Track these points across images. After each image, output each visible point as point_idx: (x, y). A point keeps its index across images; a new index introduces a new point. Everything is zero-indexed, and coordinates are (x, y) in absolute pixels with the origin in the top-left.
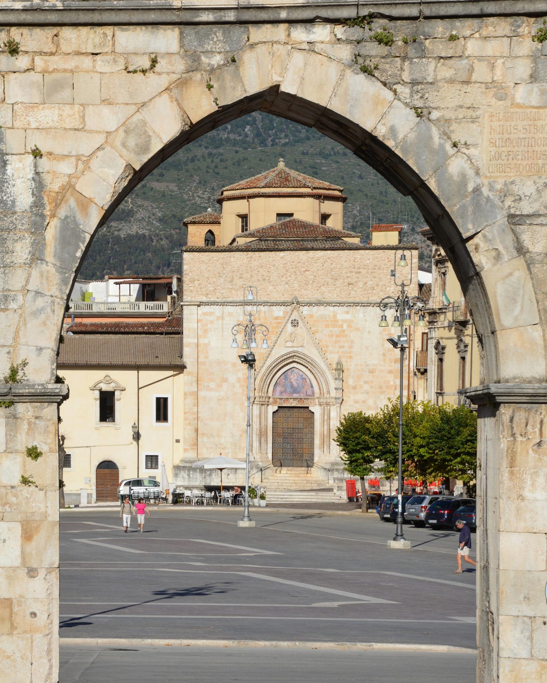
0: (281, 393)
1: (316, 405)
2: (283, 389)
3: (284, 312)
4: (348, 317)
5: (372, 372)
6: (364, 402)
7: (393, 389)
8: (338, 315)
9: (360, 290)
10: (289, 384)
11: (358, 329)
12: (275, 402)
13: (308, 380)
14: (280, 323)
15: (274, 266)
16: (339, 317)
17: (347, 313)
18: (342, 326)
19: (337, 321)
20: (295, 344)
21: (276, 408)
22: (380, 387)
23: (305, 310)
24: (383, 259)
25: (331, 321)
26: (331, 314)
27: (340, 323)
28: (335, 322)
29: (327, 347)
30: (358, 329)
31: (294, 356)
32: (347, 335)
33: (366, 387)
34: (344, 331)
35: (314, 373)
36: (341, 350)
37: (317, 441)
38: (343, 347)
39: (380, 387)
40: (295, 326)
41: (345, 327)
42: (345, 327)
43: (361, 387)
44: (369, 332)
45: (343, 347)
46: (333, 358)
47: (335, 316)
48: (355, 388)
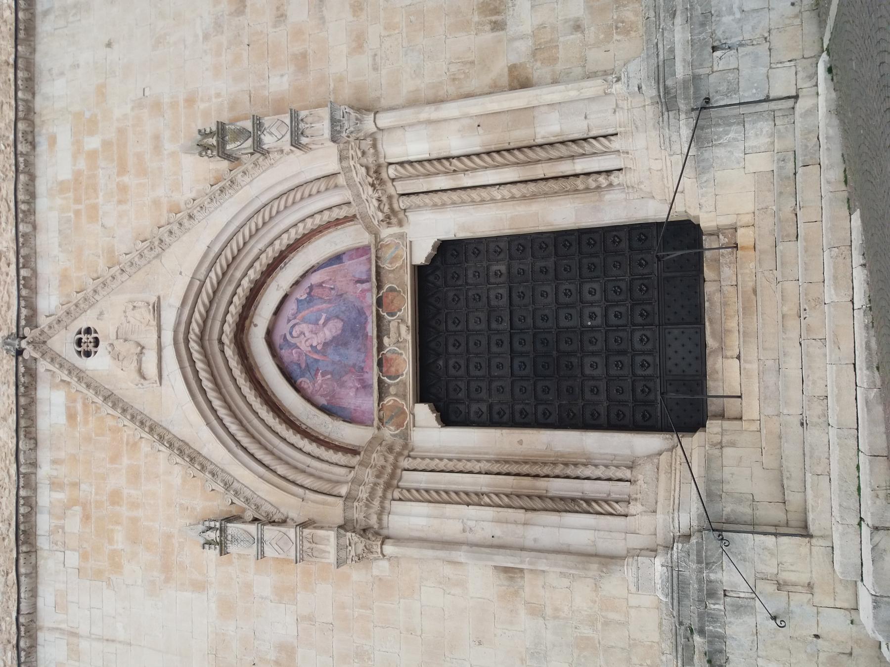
0: (365, 386)
1: (402, 236)
2: (351, 381)
3: (53, 386)
4: (64, 139)
8: (60, 178)
10: (333, 356)
11: (101, 92)
12: (399, 416)
14: (85, 405)
17: (53, 140)
18: (92, 155)
19: (78, 174)
20: (150, 340)
21: (424, 413)
23: (49, 302)
25: (77, 201)
26: (59, 201)
27: (82, 164)
28: (80, 186)
29: (156, 203)
30: (101, 92)
31: (201, 339)
32: (121, 131)
34: (106, 144)
35: (271, 253)
36: (169, 146)
37: (562, 214)
38: (157, 138)
40: (97, 342)
41: (93, 143)
42: (93, 143)
43: (298, 33)
44: (109, 45)
45: (157, 138)
47: (62, 187)
48: (301, 61)
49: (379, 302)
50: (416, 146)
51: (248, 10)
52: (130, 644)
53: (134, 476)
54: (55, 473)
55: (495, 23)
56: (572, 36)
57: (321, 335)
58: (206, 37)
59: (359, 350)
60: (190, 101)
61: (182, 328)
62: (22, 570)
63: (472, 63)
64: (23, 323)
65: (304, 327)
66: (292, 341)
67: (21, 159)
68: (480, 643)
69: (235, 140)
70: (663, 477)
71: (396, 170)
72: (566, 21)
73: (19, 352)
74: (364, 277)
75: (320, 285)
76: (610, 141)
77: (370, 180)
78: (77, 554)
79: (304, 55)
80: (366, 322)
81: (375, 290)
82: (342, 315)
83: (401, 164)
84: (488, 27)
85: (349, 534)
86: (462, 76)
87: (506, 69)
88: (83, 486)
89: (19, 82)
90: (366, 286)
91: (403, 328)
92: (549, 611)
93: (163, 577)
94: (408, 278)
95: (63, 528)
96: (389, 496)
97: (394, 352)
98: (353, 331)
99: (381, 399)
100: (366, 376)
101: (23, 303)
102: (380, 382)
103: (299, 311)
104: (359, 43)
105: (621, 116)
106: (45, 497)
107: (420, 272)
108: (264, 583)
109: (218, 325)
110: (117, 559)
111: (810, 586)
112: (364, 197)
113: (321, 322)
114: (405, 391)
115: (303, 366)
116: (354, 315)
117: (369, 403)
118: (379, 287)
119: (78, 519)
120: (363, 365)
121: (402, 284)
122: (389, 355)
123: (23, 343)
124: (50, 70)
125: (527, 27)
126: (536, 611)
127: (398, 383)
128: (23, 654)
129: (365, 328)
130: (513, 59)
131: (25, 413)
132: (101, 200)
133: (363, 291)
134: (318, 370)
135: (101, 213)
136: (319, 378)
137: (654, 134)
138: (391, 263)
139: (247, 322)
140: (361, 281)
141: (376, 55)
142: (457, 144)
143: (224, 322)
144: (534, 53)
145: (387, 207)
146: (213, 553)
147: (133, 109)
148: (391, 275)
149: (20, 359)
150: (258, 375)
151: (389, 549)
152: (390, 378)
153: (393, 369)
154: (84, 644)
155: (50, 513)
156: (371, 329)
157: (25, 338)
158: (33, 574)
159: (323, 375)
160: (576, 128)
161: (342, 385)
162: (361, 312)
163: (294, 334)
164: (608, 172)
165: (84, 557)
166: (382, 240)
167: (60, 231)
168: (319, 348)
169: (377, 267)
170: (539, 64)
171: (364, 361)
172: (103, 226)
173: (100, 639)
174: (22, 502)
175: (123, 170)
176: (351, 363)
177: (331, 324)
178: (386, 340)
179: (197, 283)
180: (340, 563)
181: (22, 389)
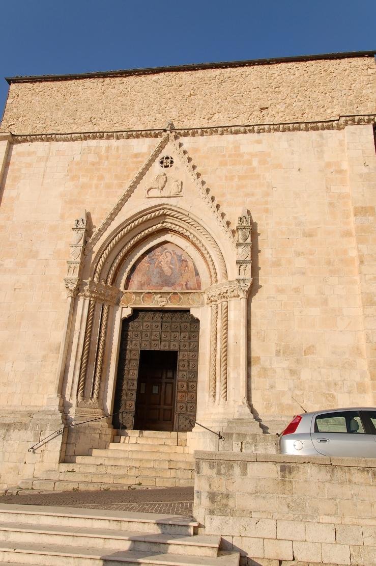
0: (142, 285)
1: (203, 304)
2: (144, 279)
4: (258, 148)
5: (310, 235)
6: (297, 290)
7: (357, 263)
8: (241, 147)
9: (281, 114)
10: (156, 270)
13: (190, 264)
15: (142, 92)
16: (243, 149)
17: (259, 142)
18: (249, 162)
20: (164, 193)
21: (127, 312)
22: (329, 263)
23: (186, 141)
24: (317, 72)
25: (230, 156)
27: (246, 157)
29: (223, 195)
33: (300, 262)
34: (253, 170)
39: (329, 263)
42: (255, 163)
46: (234, 214)
47: (237, 148)
48: (276, 264)
49: (175, 293)
50: (232, 315)
51: (305, 238)
52: (42, 185)
53: (108, 186)
54: (113, 148)
55: (279, 352)
56: (268, 385)
57: (166, 266)
58: (295, 218)
59: (157, 283)
60: (267, 211)
61: (168, 207)
62: (73, 135)
63: (264, 341)
64: (178, 131)
65: (169, 258)
66: (164, 253)
67: (251, 128)
68: (34, 335)
69: (242, 235)
70: (93, 410)
71: (225, 305)
72: (276, 383)
73: (165, 131)
74: (188, 286)
75: (187, 266)
76: (224, 397)
77: (222, 293)
78: (79, 160)
79: (279, 265)
80: (169, 286)
81: (180, 292)
82: (172, 276)
83: (227, 308)
84: (278, 348)
85: (76, 283)
86: (259, 336)
87: (258, 356)
88: (107, 162)
89: (287, 126)
90: (184, 287)
91: (163, 304)
92: (44, 363)
93: (67, 200)
94: (184, 306)
95: (90, 153)
96: (92, 299)
97: (154, 299)
98: (167, 281)
99: (134, 293)
100: (146, 286)
101: (186, 131)
102: (142, 293)
103: (177, 255)
104: (280, 291)
105: (232, 403)
106: (103, 143)
107: (187, 311)
108: (61, 245)
109: (171, 221)
110: (76, 179)
111: (42, 461)
112: (216, 290)
113: (171, 266)
114: (137, 304)
115: (153, 257)
116: (173, 281)
117: (134, 287)
118: (181, 293)
119: (93, 160)
120: (151, 284)
121: (182, 303)
122: (153, 297)
123: (168, 132)
124: (293, 140)
125: (275, 365)
126: (45, 358)
127: (140, 301)
128: (40, 136)
129: (166, 286)
130: (262, 359)
131: (139, 134)
132: (229, 167)
133: (182, 285)
134: (151, 264)
135: (223, 167)
136: (147, 265)
137: (221, 417)
138: (192, 299)
139: (173, 233)
140: (186, 285)
141: (274, 298)
142: (231, 333)
143: (172, 223)
144: (264, 369)
145: (213, 299)
146: (74, 225)
147: (267, 182)
148: (186, 299)
149: (162, 131)
150: (150, 238)
151: (70, 299)
152: (143, 297)
153: (147, 299)
154: (43, 164)
155: (97, 146)
156: (166, 289)
157: (171, 133)
158: (72, 140)
159: (149, 267)
160: (231, 385)
161: (143, 275)
162: (173, 284)
163: (167, 253)
164: (214, 396)
165: (78, 164)
166: (202, 295)
167: (217, 147)
168: (160, 265)
169: (190, 293)
170: (259, 370)
171: (152, 285)
172: (217, 168)
173: (45, 171)
174: (102, 134)
175: (240, 178)
176: (152, 279)
177: (170, 270)
178: (159, 296)
179: (187, 214)
180: (66, 280)
181: (149, 132)
